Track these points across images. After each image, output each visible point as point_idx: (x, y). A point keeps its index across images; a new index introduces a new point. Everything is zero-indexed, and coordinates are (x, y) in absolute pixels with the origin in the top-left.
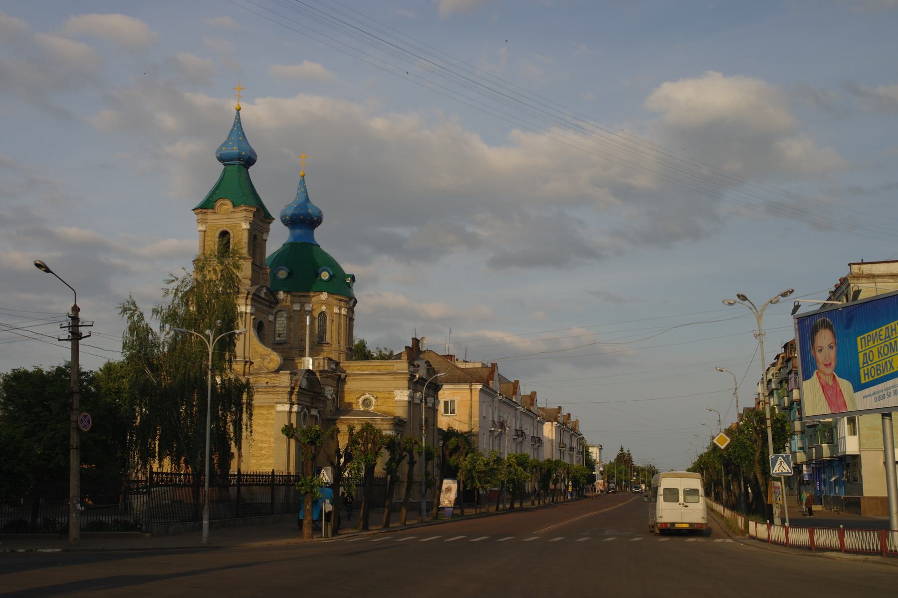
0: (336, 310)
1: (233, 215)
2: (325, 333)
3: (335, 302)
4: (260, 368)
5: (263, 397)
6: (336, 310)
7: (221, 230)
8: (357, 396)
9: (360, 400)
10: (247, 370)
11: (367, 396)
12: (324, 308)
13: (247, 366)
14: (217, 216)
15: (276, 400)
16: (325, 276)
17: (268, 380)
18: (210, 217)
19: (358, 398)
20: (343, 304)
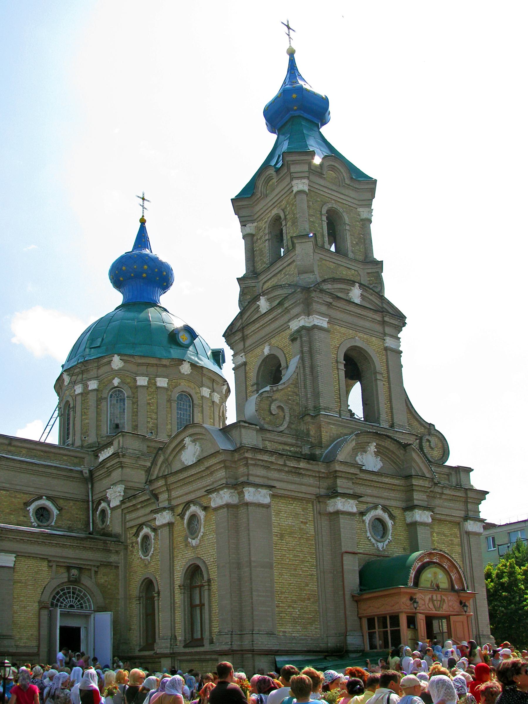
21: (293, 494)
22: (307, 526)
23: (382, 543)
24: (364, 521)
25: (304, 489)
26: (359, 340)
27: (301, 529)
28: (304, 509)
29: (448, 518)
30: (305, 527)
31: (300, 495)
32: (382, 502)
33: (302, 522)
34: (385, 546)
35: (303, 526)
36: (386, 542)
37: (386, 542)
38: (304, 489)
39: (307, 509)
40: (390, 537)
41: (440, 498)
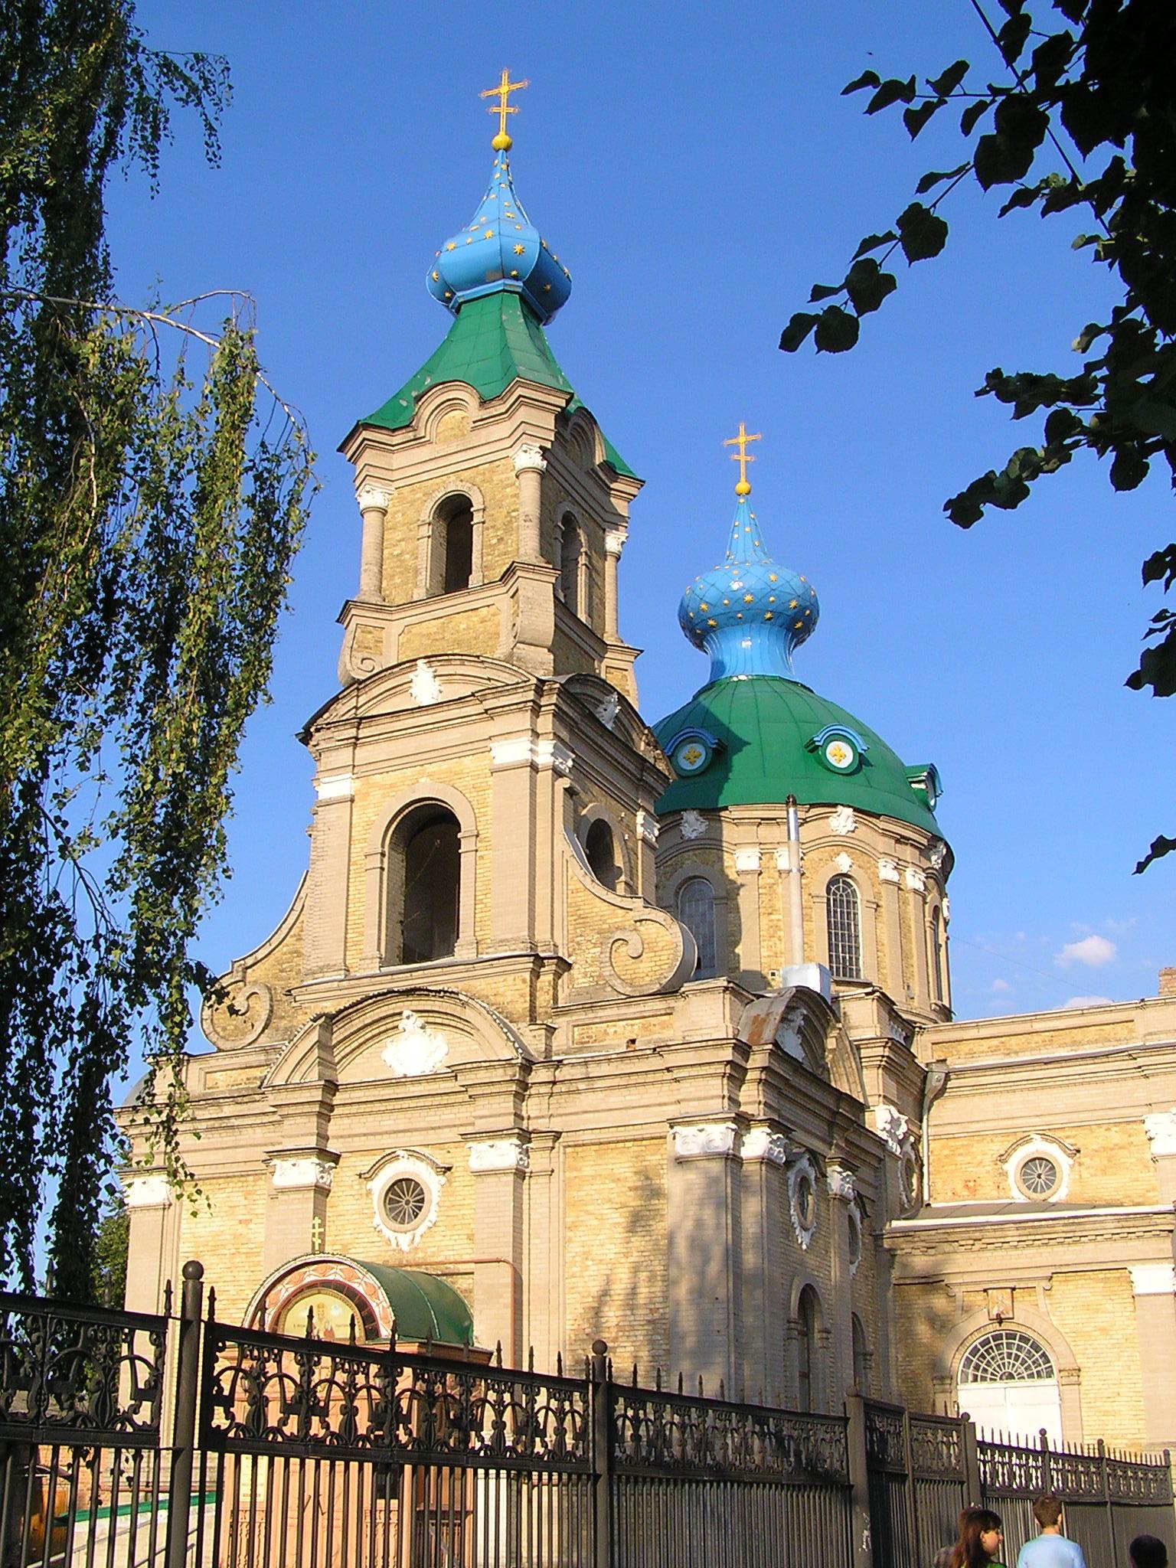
0: (887, 872)
1: (483, 435)
2: (853, 949)
3: (884, 844)
4: (601, 983)
5: (616, 1099)
6: (887, 872)
7: (439, 495)
8: (998, 1147)
9: (1013, 1165)
10: (544, 999)
11: (1038, 1147)
12: (844, 863)
13: (546, 979)
14: (423, 453)
15: (672, 1111)
16: (840, 755)
17: (634, 1029)
18: (399, 459)
19: (1002, 1159)
20: (908, 853)
21: (221, 1169)
22: (251, 1226)
23: (409, 1235)
24: (369, 1193)
25: (240, 1154)
26: (425, 786)
27: (236, 1236)
28: (247, 1194)
29: (622, 1134)
30: (246, 1231)
31: (235, 1168)
32: (403, 1140)
33: (240, 1222)
34: (417, 1239)
35: (241, 1229)
36: (422, 1229)
37: (422, 1229)
38: (240, 1154)
39: (253, 1192)
40: (432, 1216)
41: (593, 1090)
